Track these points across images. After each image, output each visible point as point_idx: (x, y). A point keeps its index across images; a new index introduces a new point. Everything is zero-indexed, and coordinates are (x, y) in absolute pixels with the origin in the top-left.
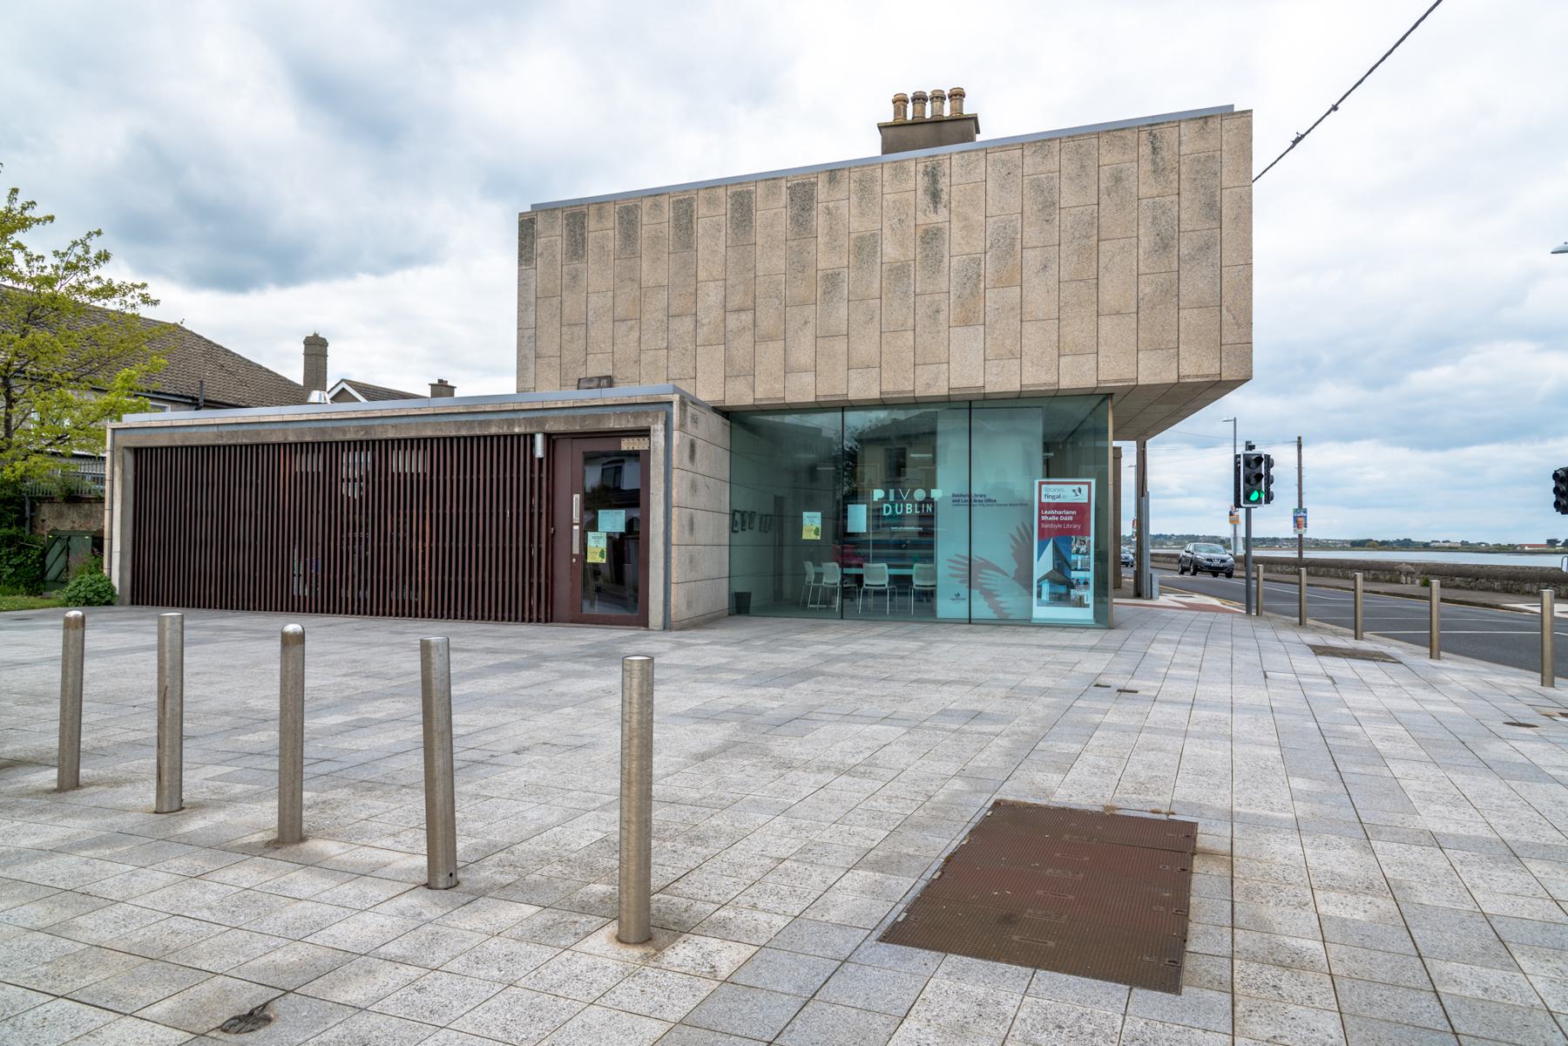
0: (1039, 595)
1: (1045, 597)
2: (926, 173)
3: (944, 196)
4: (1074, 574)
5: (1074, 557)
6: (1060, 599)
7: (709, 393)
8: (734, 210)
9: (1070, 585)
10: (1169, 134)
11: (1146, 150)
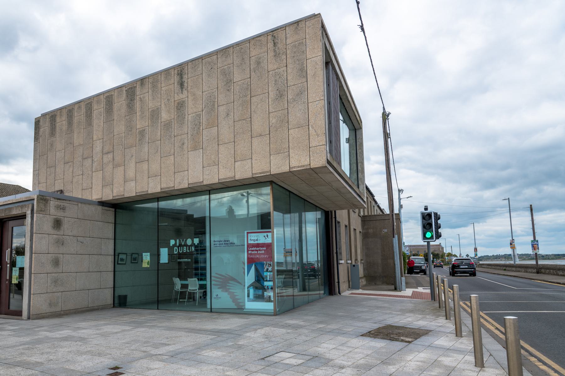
0: (248, 296)
1: (251, 296)
2: (178, 74)
3: (185, 84)
4: (266, 284)
5: (265, 274)
6: (259, 298)
7: (96, 196)
8: (106, 105)
9: (264, 289)
10: (281, 35)
11: (271, 45)
